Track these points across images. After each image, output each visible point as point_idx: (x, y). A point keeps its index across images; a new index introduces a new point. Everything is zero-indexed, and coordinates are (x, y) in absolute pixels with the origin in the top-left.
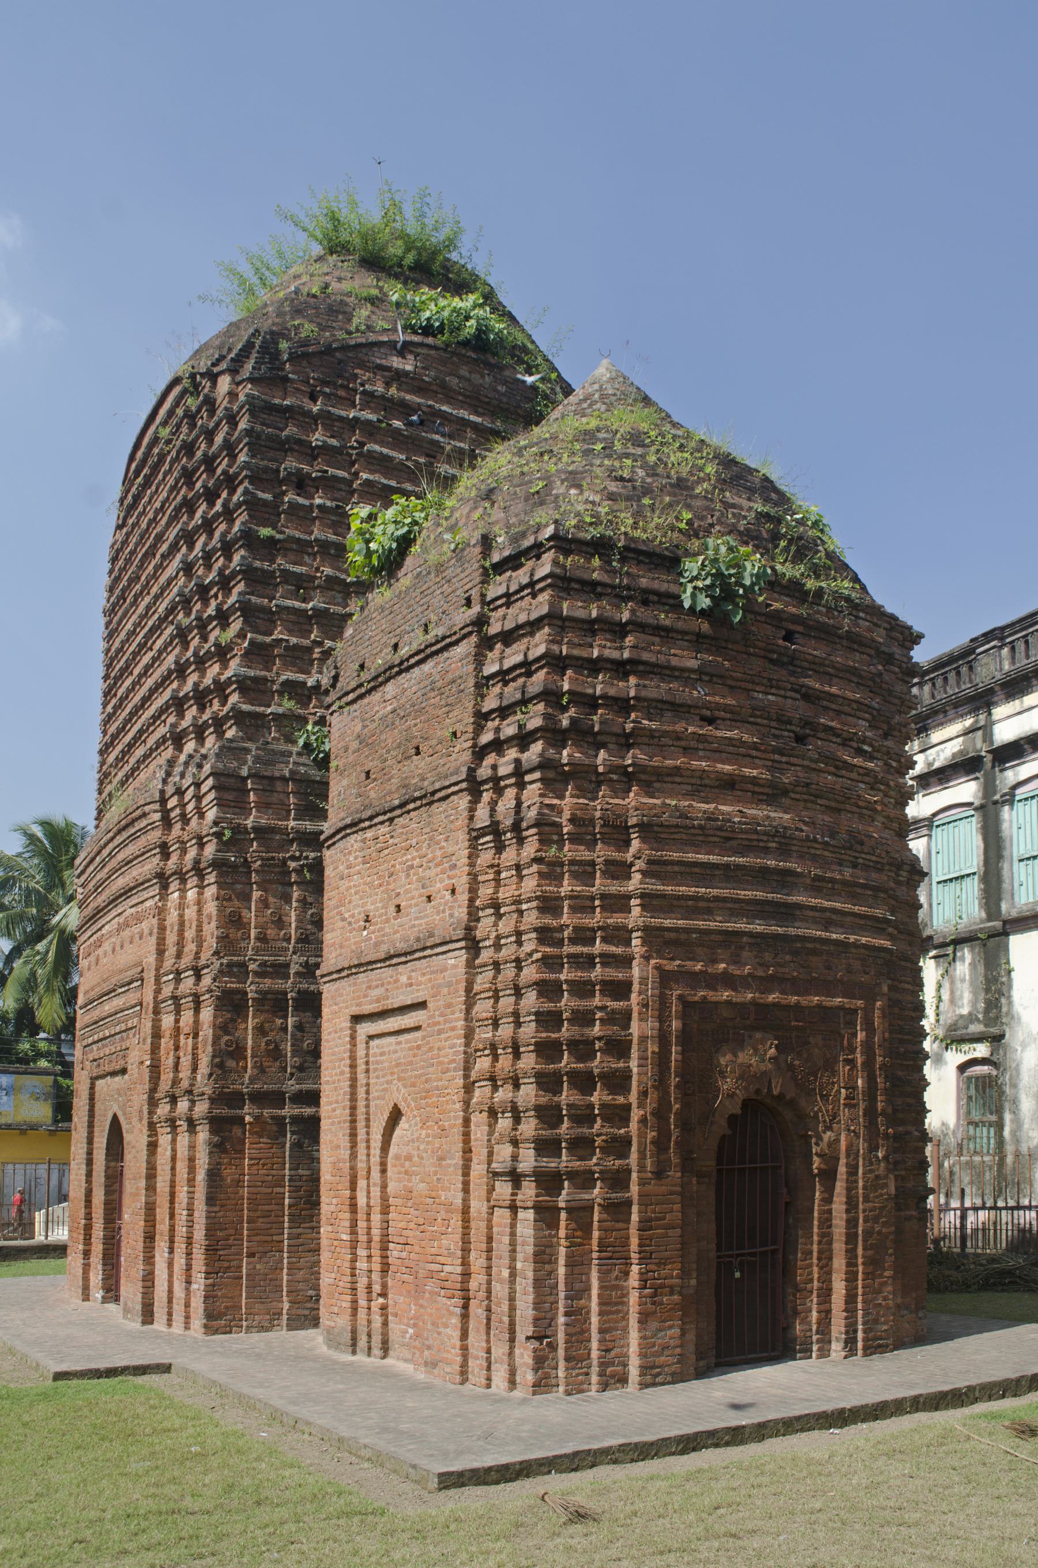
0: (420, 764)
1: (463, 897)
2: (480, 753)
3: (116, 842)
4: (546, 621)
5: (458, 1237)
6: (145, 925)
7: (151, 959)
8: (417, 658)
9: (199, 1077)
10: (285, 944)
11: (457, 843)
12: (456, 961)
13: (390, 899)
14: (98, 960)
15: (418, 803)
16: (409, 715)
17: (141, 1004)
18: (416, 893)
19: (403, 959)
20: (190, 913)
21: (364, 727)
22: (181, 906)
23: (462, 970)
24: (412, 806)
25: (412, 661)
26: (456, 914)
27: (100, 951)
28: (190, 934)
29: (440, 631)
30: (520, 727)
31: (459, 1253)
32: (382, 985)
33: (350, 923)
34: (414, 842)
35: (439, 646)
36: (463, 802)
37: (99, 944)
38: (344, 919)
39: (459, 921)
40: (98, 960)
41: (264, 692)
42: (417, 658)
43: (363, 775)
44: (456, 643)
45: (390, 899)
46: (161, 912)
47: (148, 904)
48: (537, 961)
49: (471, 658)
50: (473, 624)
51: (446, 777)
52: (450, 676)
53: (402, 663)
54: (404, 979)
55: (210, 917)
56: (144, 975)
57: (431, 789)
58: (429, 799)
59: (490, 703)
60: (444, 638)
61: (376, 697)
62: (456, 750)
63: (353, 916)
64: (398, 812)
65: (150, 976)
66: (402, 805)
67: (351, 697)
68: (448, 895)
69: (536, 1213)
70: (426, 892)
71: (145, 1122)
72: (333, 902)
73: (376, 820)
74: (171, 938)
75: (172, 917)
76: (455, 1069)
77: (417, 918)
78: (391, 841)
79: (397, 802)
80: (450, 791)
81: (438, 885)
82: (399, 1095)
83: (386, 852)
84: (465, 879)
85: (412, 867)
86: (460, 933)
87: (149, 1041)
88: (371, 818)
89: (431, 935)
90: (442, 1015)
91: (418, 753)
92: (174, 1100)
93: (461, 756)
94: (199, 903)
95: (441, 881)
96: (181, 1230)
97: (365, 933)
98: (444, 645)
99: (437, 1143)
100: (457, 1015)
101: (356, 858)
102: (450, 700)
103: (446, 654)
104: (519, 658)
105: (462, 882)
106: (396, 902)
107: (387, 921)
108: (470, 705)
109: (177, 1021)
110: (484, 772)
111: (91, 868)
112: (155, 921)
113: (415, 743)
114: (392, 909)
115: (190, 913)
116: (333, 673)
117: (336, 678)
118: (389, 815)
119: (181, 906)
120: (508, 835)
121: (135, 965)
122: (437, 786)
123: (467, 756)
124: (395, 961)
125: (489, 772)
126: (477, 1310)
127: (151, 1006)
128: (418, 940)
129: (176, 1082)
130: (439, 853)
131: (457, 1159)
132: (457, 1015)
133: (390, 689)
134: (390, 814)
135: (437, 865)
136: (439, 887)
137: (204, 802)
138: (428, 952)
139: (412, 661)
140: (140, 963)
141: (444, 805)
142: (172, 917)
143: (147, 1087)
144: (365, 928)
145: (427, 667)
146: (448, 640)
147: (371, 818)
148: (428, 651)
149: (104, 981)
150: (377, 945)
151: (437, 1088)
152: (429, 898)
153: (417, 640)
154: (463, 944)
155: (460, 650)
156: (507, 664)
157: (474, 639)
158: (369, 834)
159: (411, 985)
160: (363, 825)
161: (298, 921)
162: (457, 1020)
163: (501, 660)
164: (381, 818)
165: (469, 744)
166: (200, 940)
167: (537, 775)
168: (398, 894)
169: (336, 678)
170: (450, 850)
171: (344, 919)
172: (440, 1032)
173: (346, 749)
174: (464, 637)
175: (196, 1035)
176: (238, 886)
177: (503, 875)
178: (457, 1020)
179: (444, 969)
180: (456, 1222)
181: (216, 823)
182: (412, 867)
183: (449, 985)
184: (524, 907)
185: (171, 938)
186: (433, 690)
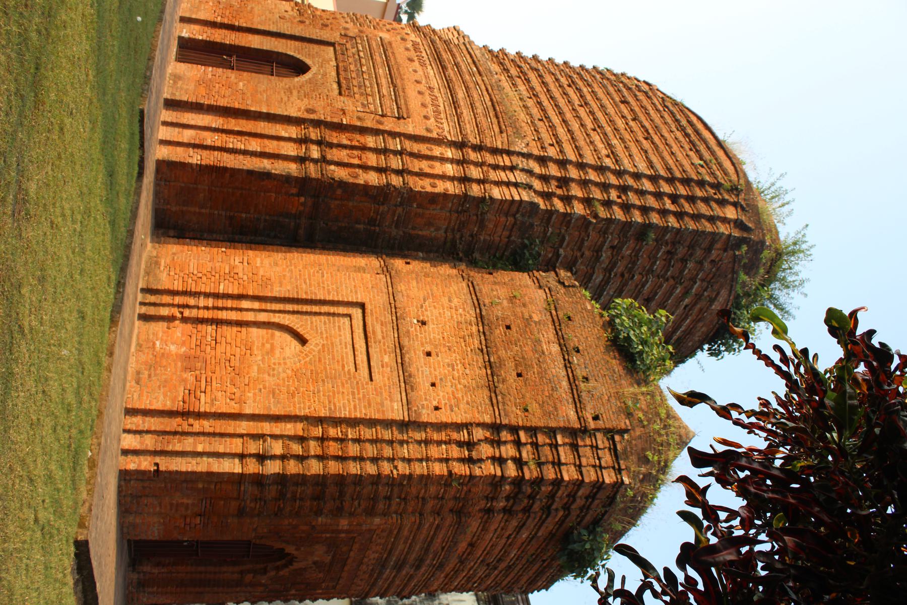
0: (511, 377)
1: (433, 418)
2: (514, 430)
3: (485, 93)
4: (580, 478)
5: (224, 410)
6: (432, 122)
7: (410, 128)
8: (571, 375)
9: (332, 167)
10: (410, 227)
11: (465, 413)
12: (396, 411)
13: (436, 346)
14: (411, 60)
15: (490, 379)
16: (541, 367)
17: (382, 116)
18: (437, 373)
19: (399, 361)
20: (438, 168)
21: (536, 323)
22: (443, 160)
23: (390, 416)
24: (489, 372)
25: (569, 370)
26: (424, 411)
27: (416, 64)
28: (424, 165)
29: (584, 394)
30: (526, 463)
31: (213, 410)
32: (383, 338)
33: (422, 307)
34: (468, 371)
35: (576, 396)
36: (487, 419)
37: (423, 65)
38: (425, 300)
39: (419, 415)
40: (411, 60)
41: (561, 224)
42: (571, 375)
43: (508, 323)
44: (577, 412)
45: (436, 346)
46: (439, 142)
47: (445, 126)
48: (392, 472)
49: (567, 425)
50: (585, 427)
51: (504, 403)
52: (559, 405)
53: (569, 362)
54: (386, 359)
55: (434, 186)
56: (402, 121)
57: (498, 392)
58: (493, 389)
59: (541, 439)
60: (580, 402)
61: (551, 335)
62: (518, 411)
63: (426, 310)
64: (487, 359)
65: (400, 128)
66: (489, 361)
67: (554, 312)
68: (435, 403)
69: (238, 474)
70: (438, 382)
71: (306, 116)
72: (435, 288)
73: (483, 337)
74: (423, 148)
75: (437, 151)
76: (330, 409)
77: (423, 373)
78: (469, 349)
79: (492, 360)
80: (496, 408)
81: (441, 394)
82: (315, 342)
83: (463, 344)
84: (444, 420)
85: (453, 370)
86: (413, 419)
87: (359, 124)
88: (484, 333)
89: (412, 389)
90: (364, 396)
91: (519, 375)
92: (319, 143)
93: (515, 417)
94: (443, 177)
95: (444, 396)
96: (233, 142)
97: (415, 321)
98: (578, 402)
99: (284, 389)
100: (364, 411)
101: (461, 315)
102: (545, 404)
103: (571, 400)
104: (563, 460)
105: (444, 416)
106: (433, 354)
107: (422, 344)
108: (541, 424)
109: (370, 149)
110: (505, 435)
111: (470, 60)
112: (434, 135)
113: (524, 373)
114: (428, 349)
115: (438, 168)
116: (567, 284)
117: (563, 284)
118: (485, 350)
119: (443, 160)
120: (466, 453)
121: (408, 113)
122: (499, 398)
123: (514, 422)
124: (398, 351)
125: (503, 439)
126: (173, 424)
127: (381, 127)
128: (410, 376)
129: (331, 145)
130: (460, 396)
131: (275, 410)
132: (364, 411)
133: (555, 348)
134: (486, 349)
135: (453, 392)
136: (440, 396)
137: (504, 188)
138: (403, 385)
139: (569, 370)
140: (408, 117)
141: (487, 401)
142: (437, 151)
143: (329, 119)
144: (418, 321)
145: (565, 384)
146: (578, 405)
147: (484, 333)
148: (574, 387)
149: (398, 69)
150: (408, 332)
151: (319, 391)
152: (433, 385)
153: (580, 373)
154: (407, 419)
155: (572, 414)
156: (561, 449)
157: (577, 426)
158: (474, 328)
159: (383, 367)
160: (480, 324)
161: (423, 236)
162: (361, 412)
163: (564, 444)
164: (484, 342)
165: (521, 424)
166: (421, 174)
167: (499, 473)
168: (438, 356)
169: (563, 284)
170: (462, 406)
171: (425, 300)
172: (353, 393)
173: (524, 305)
174: (579, 418)
175: (359, 166)
176: (450, 205)
177: (444, 446)
178: (361, 412)
179: (391, 401)
180: (234, 408)
181: (491, 198)
182: (453, 370)
183: (382, 404)
184: (424, 464)
185: (423, 148)
186: (552, 390)
